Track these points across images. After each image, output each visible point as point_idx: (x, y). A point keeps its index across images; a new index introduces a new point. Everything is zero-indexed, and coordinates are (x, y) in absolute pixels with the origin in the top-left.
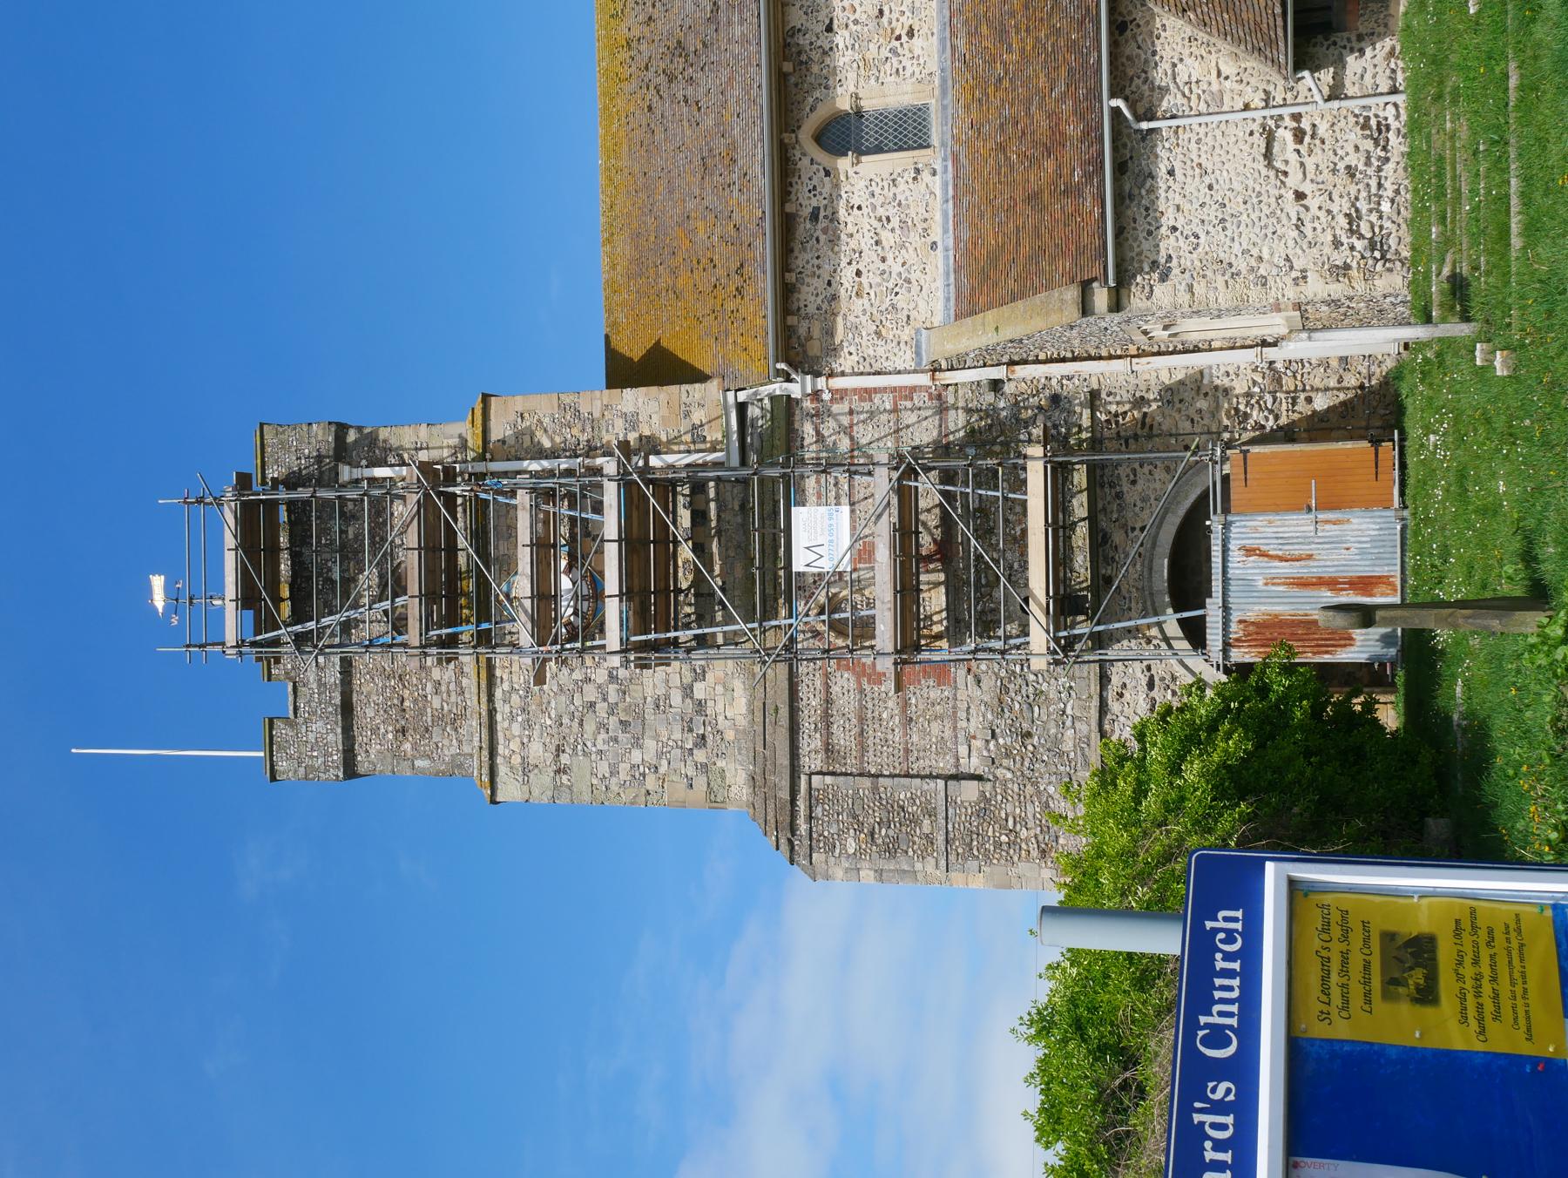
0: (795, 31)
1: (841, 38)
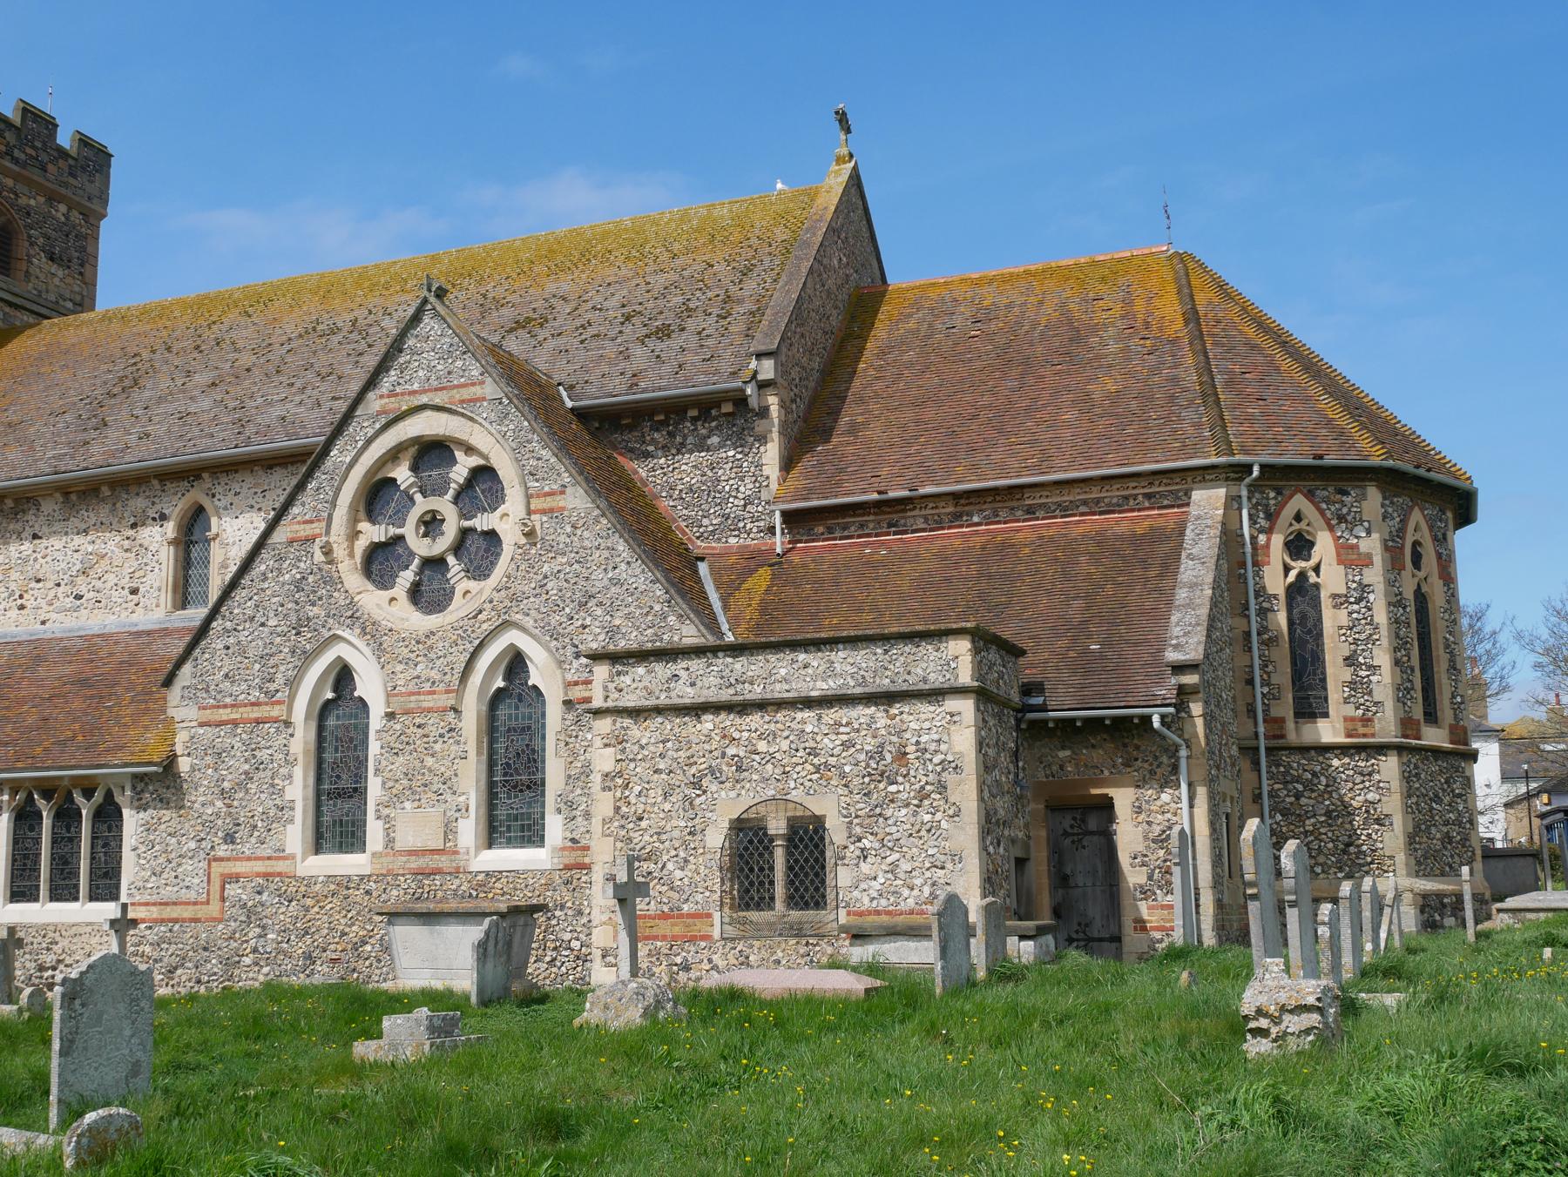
0: (38, 506)
1: (27, 547)
